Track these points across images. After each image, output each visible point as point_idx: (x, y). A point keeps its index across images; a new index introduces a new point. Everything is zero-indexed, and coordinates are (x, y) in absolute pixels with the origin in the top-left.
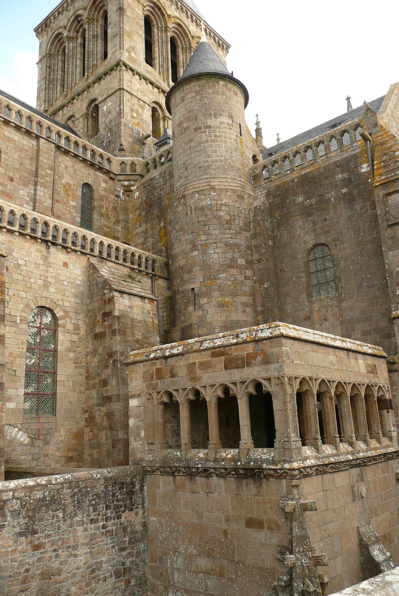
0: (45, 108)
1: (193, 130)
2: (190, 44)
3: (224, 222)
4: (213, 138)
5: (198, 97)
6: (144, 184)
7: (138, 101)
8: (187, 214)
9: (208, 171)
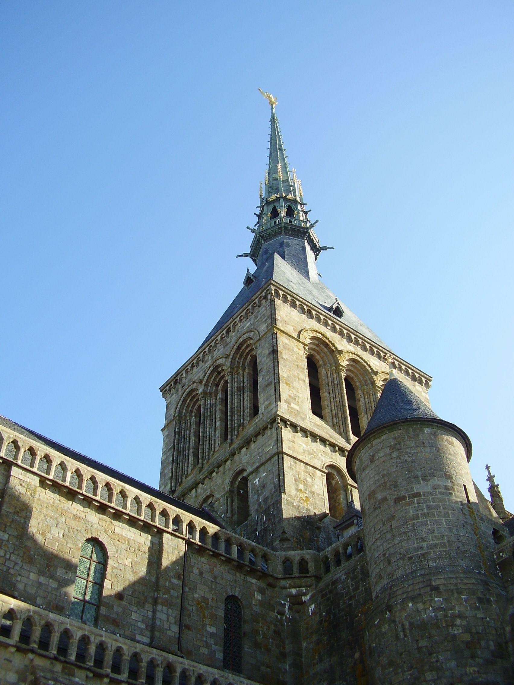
0: (171, 488)
1: (392, 503)
3: (463, 646)
4: (425, 511)
5: (394, 455)
6: (321, 590)
7: (306, 468)
8: (397, 637)
9: (425, 563)
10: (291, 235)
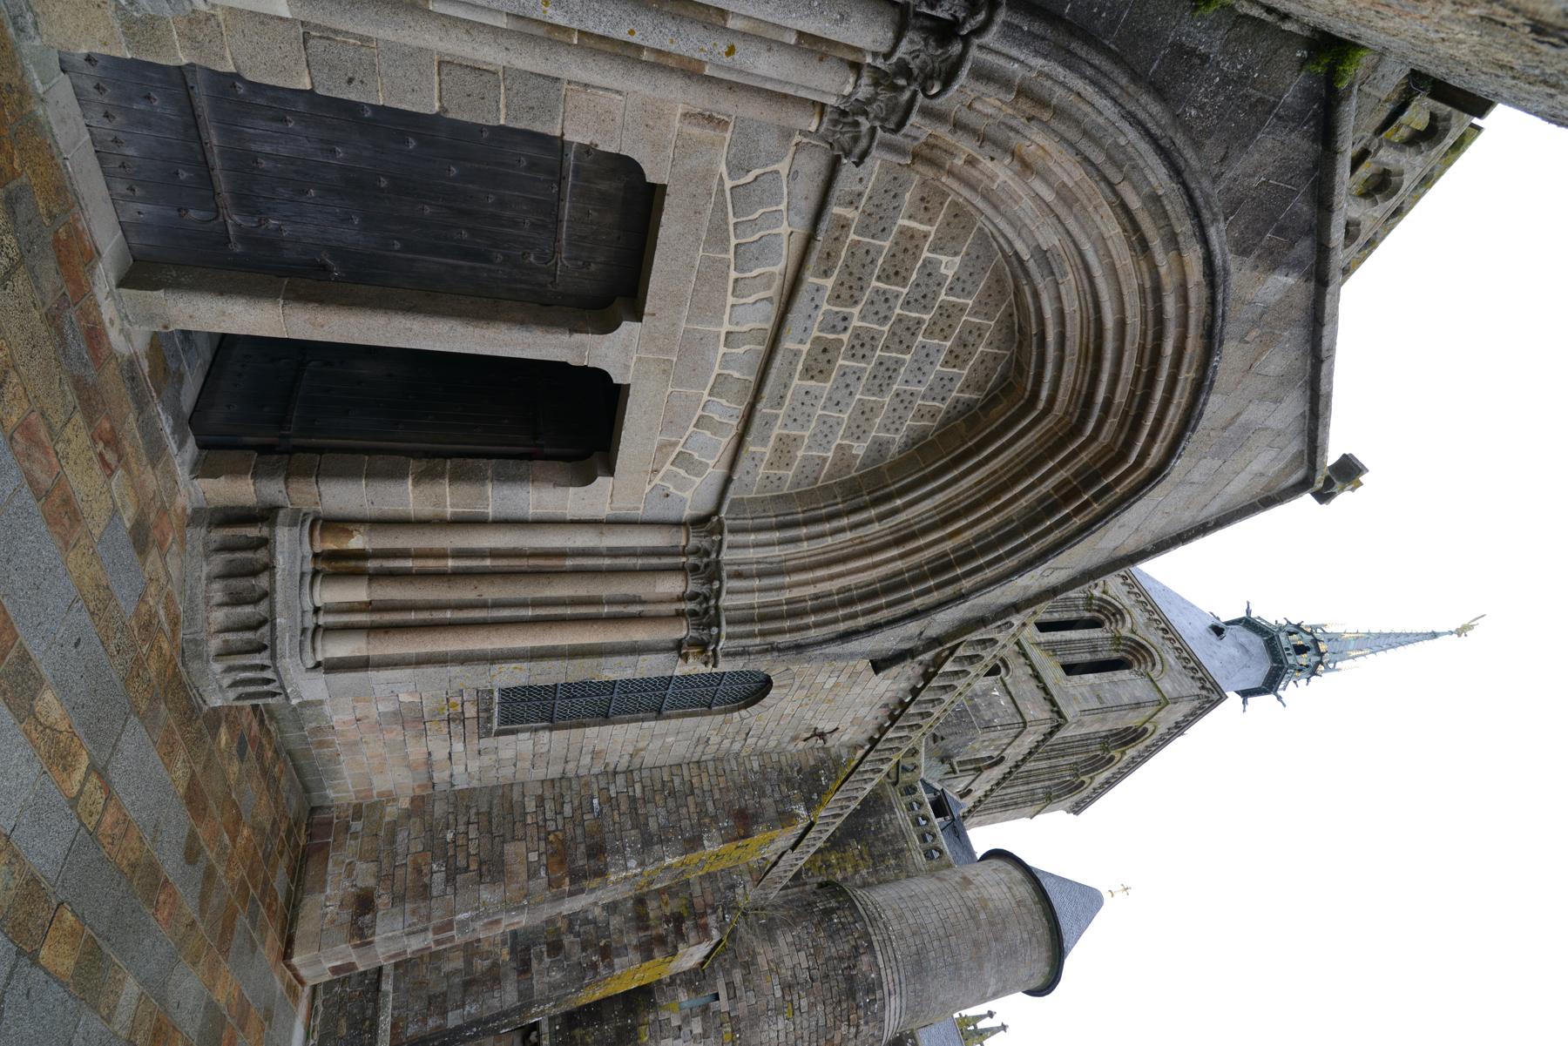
2: (1084, 774)
5: (1026, 936)
10: (1270, 673)
